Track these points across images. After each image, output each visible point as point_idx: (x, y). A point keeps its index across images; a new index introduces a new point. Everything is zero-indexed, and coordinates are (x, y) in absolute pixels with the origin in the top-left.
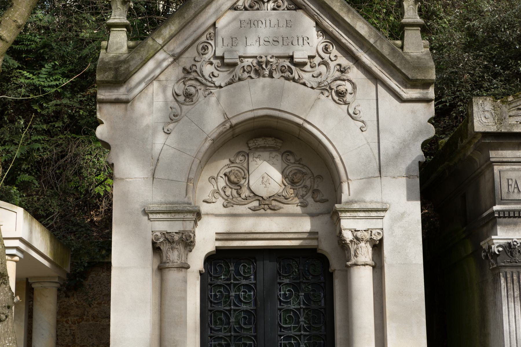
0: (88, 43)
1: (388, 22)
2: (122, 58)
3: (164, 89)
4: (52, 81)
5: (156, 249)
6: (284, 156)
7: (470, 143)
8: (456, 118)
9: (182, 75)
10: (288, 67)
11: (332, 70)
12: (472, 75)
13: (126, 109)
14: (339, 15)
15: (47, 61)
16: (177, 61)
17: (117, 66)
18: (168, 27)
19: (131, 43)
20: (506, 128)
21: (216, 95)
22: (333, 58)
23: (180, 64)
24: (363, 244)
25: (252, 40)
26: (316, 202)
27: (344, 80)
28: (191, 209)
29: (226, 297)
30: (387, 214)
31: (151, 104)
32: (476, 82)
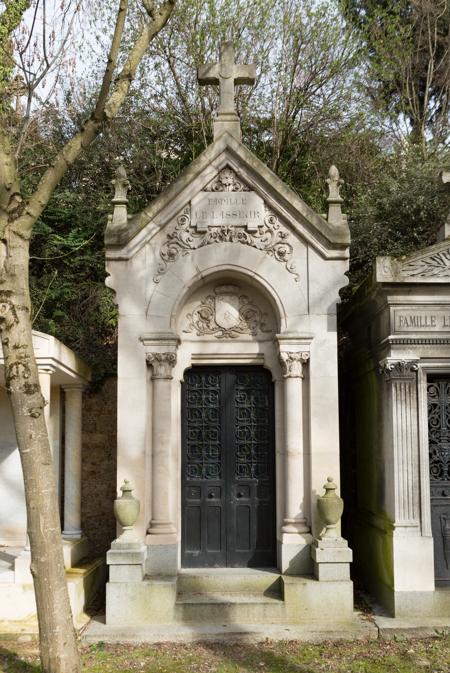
2: (123, 227)
3: (154, 251)
5: (149, 365)
7: (374, 290)
8: (367, 270)
9: (167, 240)
12: (380, 239)
13: (127, 265)
19: (130, 216)
20: (400, 280)
21: (191, 255)
22: (276, 227)
23: (165, 231)
24: (295, 362)
25: (217, 214)
27: (284, 244)
29: (199, 399)
31: (144, 261)
32: (382, 244)
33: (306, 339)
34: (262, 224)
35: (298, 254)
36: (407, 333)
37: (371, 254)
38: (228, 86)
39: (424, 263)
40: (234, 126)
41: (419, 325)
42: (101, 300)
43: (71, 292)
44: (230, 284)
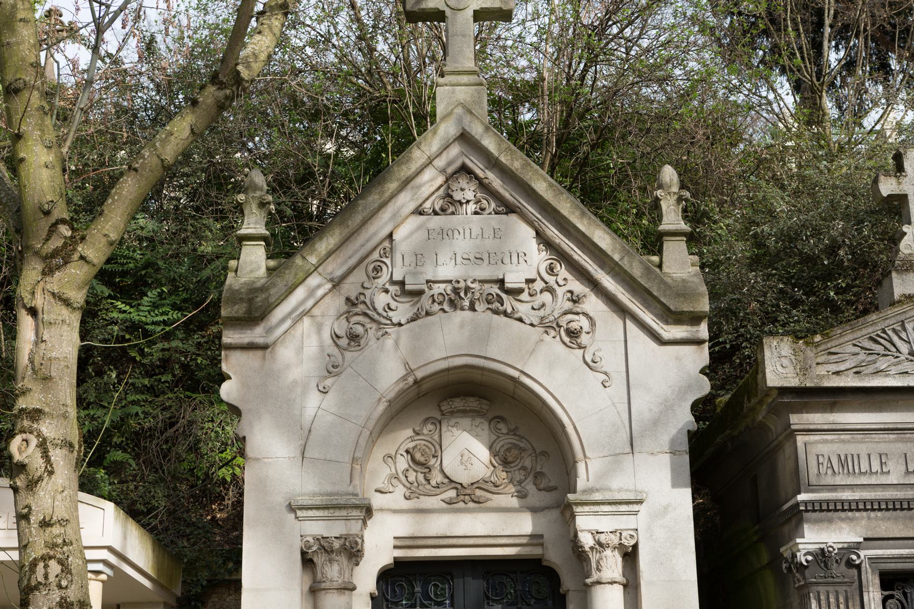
0: (210, 262)
1: (640, 227)
2: (258, 284)
3: (319, 328)
4: (157, 315)
5: (307, 561)
6: (492, 423)
7: (761, 402)
8: (741, 364)
9: (345, 308)
10: (497, 295)
12: (762, 304)
13: (264, 358)
14: (569, 221)
15: (150, 286)
16: (337, 288)
17: (251, 296)
18: (325, 239)
20: (812, 382)
21: (393, 336)
22: (561, 282)
23: (342, 292)
24: (608, 552)
25: (445, 257)
26: (540, 490)
27: (577, 314)
28: (357, 502)
30: (642, 508)
31: (300, 350)
32: (767, 313)
34: (533, 275)
35: (607, 333)
36: (834, 488)
37: (748, 332)
38: (463, 25)
39: (857, 350)
40: (476, 95)
41: (857, 471)
42: (202, 428)
43: (143, 412)
44: (472, 395)
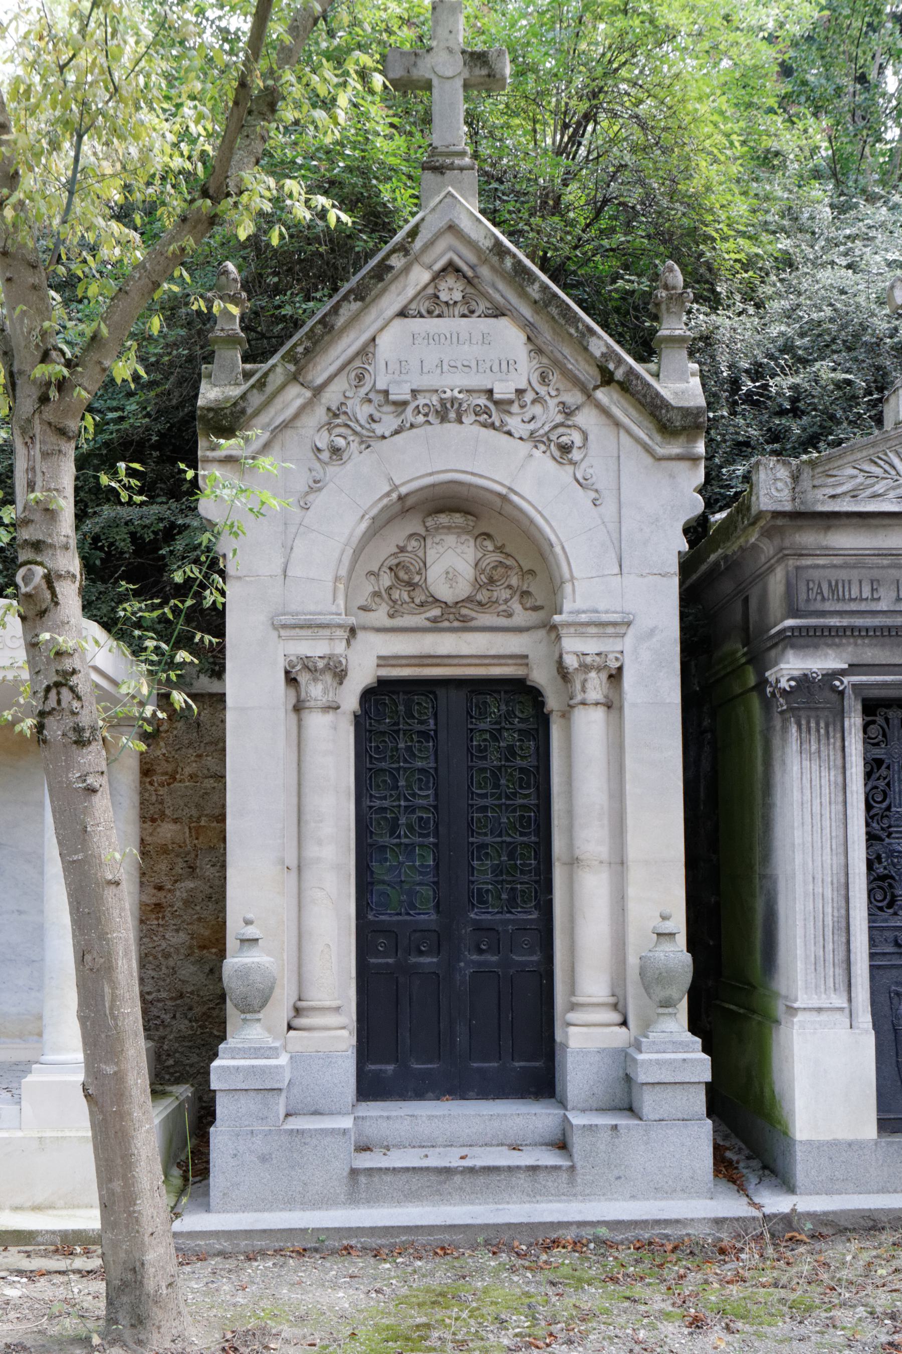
5: (291, 680)
6: (479, 540)
11: (551, 412)
22: (553, 393)
24: (593, 674)
26: (526, 609)
27: (569, 426)
29: (392, 750)
30: (631, 632)
33: (614, 624)
34: (523, 385)
36: (823, 614)
39: (855, 472)
41: (847, 597)
44: (458, 510)
